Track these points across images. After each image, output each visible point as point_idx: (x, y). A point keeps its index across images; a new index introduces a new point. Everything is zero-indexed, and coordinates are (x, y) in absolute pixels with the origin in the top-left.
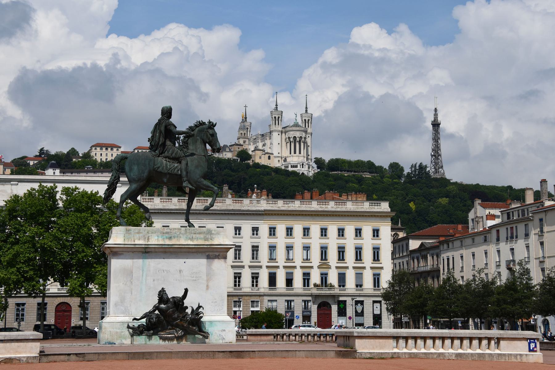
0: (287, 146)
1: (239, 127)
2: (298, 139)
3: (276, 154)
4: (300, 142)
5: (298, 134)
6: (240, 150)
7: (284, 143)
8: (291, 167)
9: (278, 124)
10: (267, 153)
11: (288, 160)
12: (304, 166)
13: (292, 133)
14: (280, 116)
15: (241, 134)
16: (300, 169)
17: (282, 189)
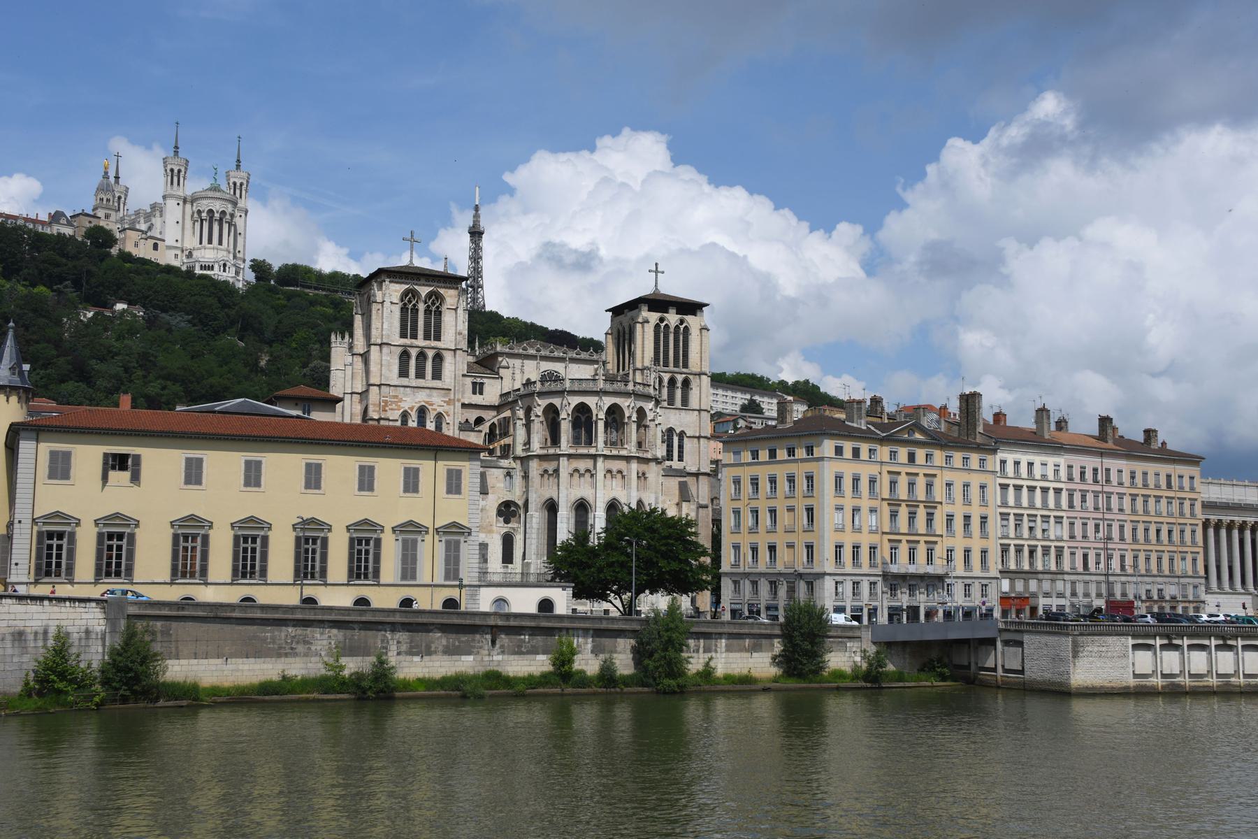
0: (194, 228)
1: (96, 186)
2: (217, 216)
3: (168, 243)
4: (220, 221)
5: (217, 206)
6: (92, 225)
7: (189, 223)
8: (201, 269)
9: (179, 184)
10: (151, 238)
11: (194, 256)
12: (227, 268)
13: (205, 202)
14: (183, 169)
15: (102, 200)
16: (220, 273)
17: (173, 299)
